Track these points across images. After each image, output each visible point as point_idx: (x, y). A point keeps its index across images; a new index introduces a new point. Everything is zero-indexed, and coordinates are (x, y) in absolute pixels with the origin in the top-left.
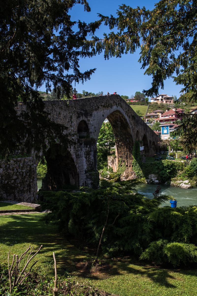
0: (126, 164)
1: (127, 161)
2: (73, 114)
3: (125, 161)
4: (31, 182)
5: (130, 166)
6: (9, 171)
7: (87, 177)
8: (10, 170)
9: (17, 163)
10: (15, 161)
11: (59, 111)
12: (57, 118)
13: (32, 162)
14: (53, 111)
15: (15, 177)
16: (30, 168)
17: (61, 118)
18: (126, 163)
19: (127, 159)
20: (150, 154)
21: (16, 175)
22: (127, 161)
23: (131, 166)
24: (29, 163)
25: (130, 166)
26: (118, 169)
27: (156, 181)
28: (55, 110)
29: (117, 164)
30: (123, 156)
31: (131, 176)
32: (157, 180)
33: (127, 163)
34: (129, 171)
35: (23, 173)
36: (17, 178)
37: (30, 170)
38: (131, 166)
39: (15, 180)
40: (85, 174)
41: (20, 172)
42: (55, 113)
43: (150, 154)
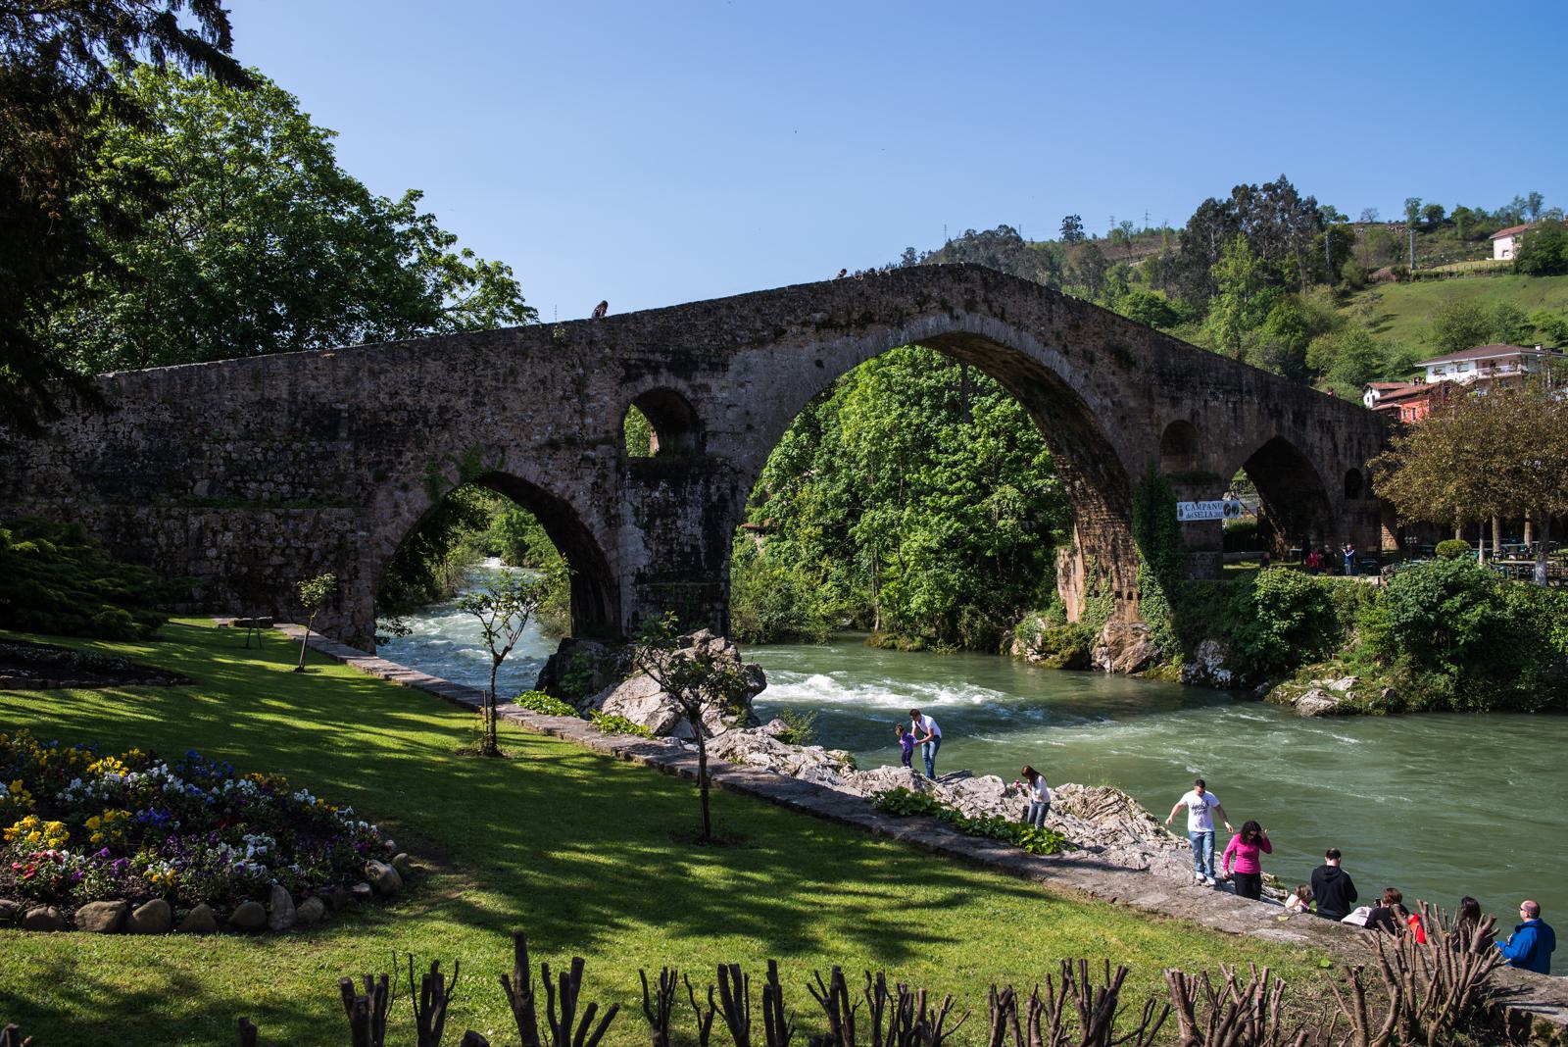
0: (1115, 585)
1: (1118, 572)
2: (596, 371)
3: (1108, 568)
4: (344, 581)
5: (1130, 597)
6: (257, 541)
7: (641, 596)
8: (261, 537)
9: (286, 523)
10: (278, 517)
11: (509, 364)
12: (497, 389)
13: (351, 523)
14: (476, 367)
15: (277, 560)
16: (339, 540)
17: (520, 386)
18: (1115, 580)
19: (1116, 563)
21: (283, 554)
22: (1118, 572)
23: (1135, 596)
24: (338, 526)
25: (1130, 597)
26: (1083, 608)
27: (1221, 674)
28: (486, 362)
29: (1080, 585)
30: (1100, 547)
31: (1132, 644)
32: (1224, 666)
33: (1119, 579)
34: (1126, 618)
35: (310, 552)
36: (287, 565)
37: (339, 547)
38: (1135, 596)
39: (278, 568)
40: (634, 585)
41: (297, 549)
42: (489, 372)
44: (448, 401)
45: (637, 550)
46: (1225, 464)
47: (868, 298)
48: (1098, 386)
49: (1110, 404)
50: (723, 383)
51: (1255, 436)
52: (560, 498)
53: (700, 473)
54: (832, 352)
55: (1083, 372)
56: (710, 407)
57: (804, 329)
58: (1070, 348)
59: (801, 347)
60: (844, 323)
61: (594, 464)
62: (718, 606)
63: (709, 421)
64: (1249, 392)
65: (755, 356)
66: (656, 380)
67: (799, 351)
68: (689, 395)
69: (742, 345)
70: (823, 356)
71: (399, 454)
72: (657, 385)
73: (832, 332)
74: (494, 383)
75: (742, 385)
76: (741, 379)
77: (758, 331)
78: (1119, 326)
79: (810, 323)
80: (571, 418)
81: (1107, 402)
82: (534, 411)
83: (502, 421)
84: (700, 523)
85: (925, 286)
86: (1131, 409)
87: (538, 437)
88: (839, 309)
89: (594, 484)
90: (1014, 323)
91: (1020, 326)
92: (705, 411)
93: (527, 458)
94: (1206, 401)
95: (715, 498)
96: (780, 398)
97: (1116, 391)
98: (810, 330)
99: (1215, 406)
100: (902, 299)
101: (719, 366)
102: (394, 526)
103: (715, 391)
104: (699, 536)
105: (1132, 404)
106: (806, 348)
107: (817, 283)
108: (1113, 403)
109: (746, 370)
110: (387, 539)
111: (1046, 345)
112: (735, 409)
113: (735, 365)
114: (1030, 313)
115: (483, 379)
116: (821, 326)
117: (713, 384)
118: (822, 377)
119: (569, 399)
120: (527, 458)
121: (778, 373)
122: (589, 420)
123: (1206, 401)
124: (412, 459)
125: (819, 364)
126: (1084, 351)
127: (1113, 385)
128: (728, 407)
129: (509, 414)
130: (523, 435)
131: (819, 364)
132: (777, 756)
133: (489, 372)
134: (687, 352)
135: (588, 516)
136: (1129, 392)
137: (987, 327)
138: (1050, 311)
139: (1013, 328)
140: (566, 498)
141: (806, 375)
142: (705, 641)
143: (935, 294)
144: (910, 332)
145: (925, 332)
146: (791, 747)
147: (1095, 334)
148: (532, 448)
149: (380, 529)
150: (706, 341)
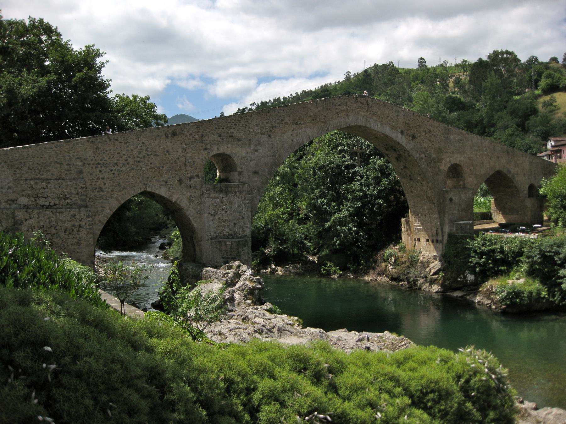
12: (148, 155)
17: (157, 154)
20: (526, 218)
27: (470, 276)
43: (526, 218)
44: (126, 160)
45: (210, 225)
46: (475, 182)
49: (424, 156)
50: (248, 150)
51: (488, 170)
52: (176, 202)
58: (405, 132)
59: (284, 133)
61: (190, 187)
64: (486, 150)
66: (218, 149)
67: (283, 135)
71: (105, 184)
72: (218, 152)
73: (298, 126)
74: (146, 152)
75: (256, 151)
76: (256, 148)
80: (180, 167)
81: (423, 156)
82: (164, 164)
83: (150, 169)
87: (166, 176)
89: (191, 196)
93: (161, 185)
97: (426, 151)
100: (329, 111)
102: (103, 215)
105: (434, 156)
106: (286, 134)
108: (425, 156)
110: (100, 221)
114: (388, 116)
115: (141, 151)
119: (178, 158)
120: (161, 185)
121: (273, 144)
122: (188, 168)
124: (111, 186)
127: (425, 148)
128: (251, 160)
129: (152, 166)
130: (159, 175)
132: (266, 319)
133: (144, 148)
135: (188, 210)
140: (178, 202)
142: (238, 267)
146: (273, 315)
148: (163, 181)
149: (97, 217)
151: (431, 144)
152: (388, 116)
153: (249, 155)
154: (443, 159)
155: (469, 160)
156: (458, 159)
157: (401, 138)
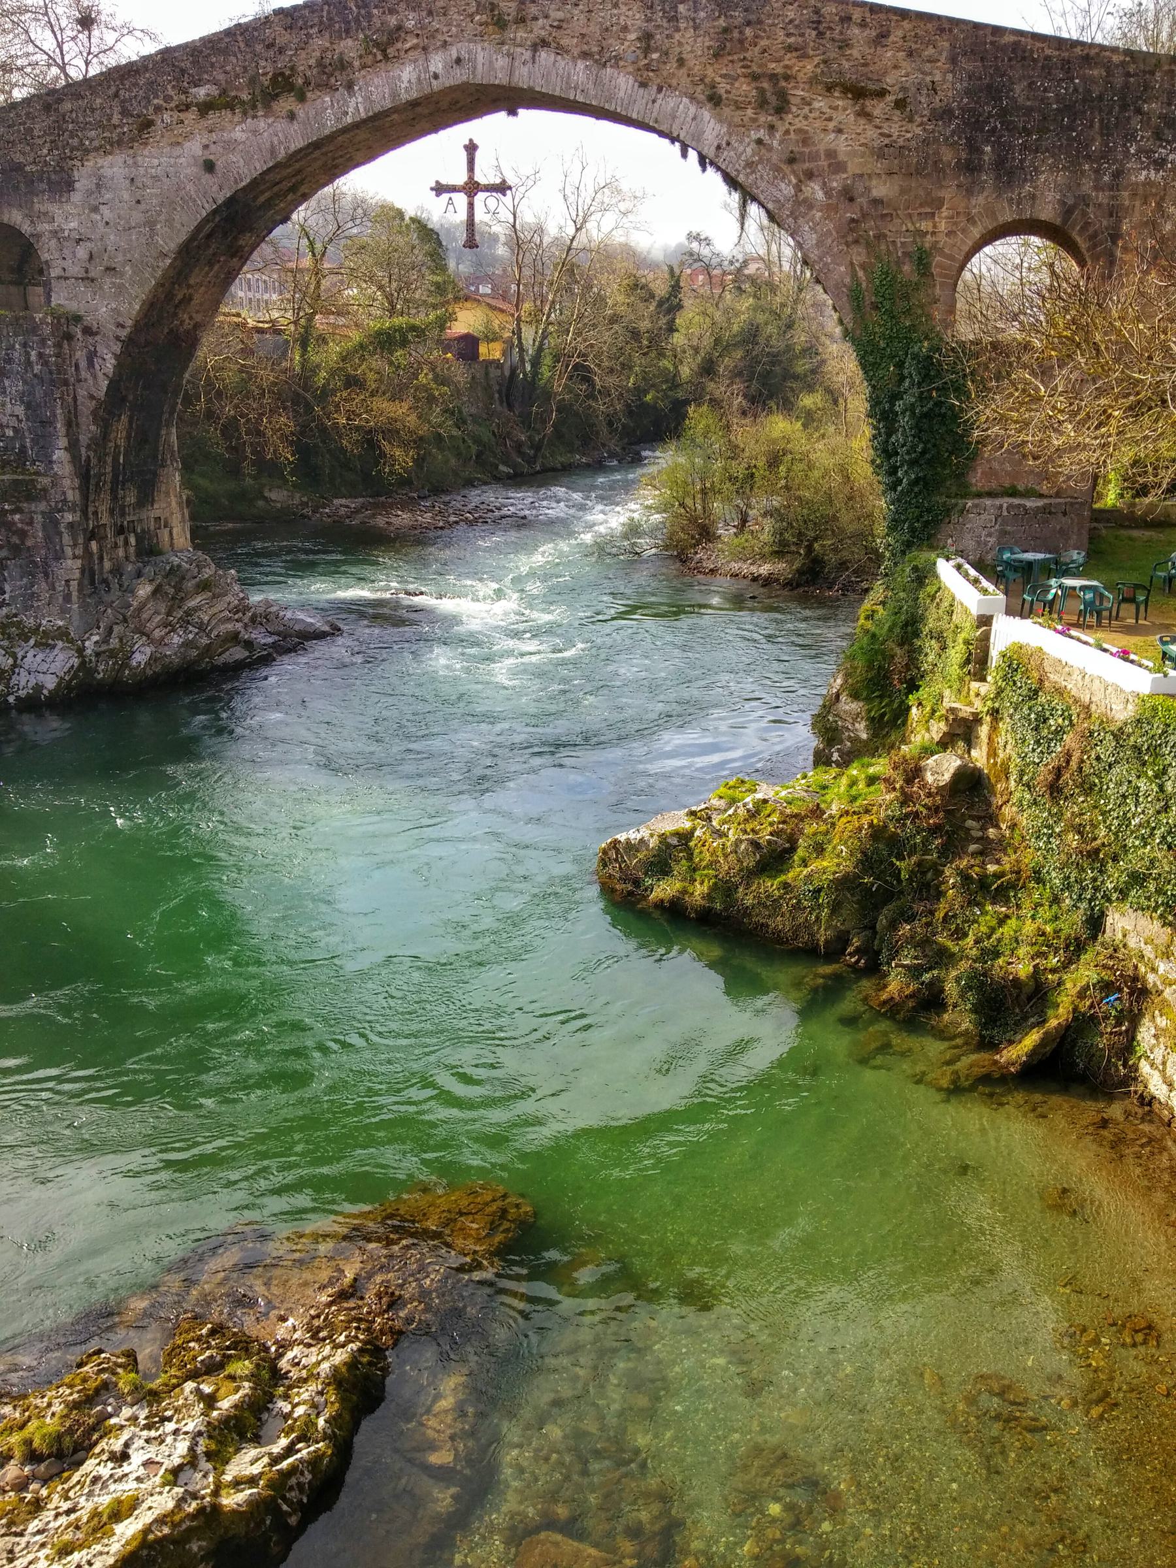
47: (281, 51)
48: (791, 161)
49: (820, 195)
50: (68, 207)
53: (16, 335)
54: (230, 146)
55: (754, 135)
56: (53, 242)
57: (182, 116)
58: (723, 87)
60: (245, 97)
62: (43, 506)
63: (54, 264)
65: (114, 166)
67: (177, 151)
68: (26, 228)
69: (87, 151)
70: (215, 153)
75: (95, 209)
77: (115, 127)
78: (863, 25)
79: (187, 107)
84: (22, 402)
85: (392, 11)
86: (876, 202)
88: (237, 76)
90: (585, 55)
91: (599, 57)
92: (48, 251)
94: (1117, 175)
95: (37, 368)
96: (151, 224)
98: (190, 116)
99: (1148, 183)
100: (350, 42)
101: (63, 185)
103: (59, 220)
104: (22, 417)
105: (881, 189)
106: (187, 145)
107: (201, 39)
108: (828, 194)
109: (98, 185)
111: (660, 90)
112: (88, 244)
113: (84, 181)
114: (625, 29)
116: (205, 108)
117: (54, 209)
118: (215, 188)
123: (1117, 175)
125: (209, 167)
126: (762, 91)
127: (831, 154)
131: (209, 167)
134: (19, 168)
136: (879, 166)
137: (524, 70)
138: (674, 19)
139: (581, 65)
141: (190, 187)
143: (410, 24)
144: (367, 99)
145: (394, 94)
147: (790, 49)
150: (45, 151)
151: (871, 133)
152: (625, 29)
153: (72, 225)
154: (939, 203)
155: (1134, 195)
156: (1051, 196)
157: (694, 119)
